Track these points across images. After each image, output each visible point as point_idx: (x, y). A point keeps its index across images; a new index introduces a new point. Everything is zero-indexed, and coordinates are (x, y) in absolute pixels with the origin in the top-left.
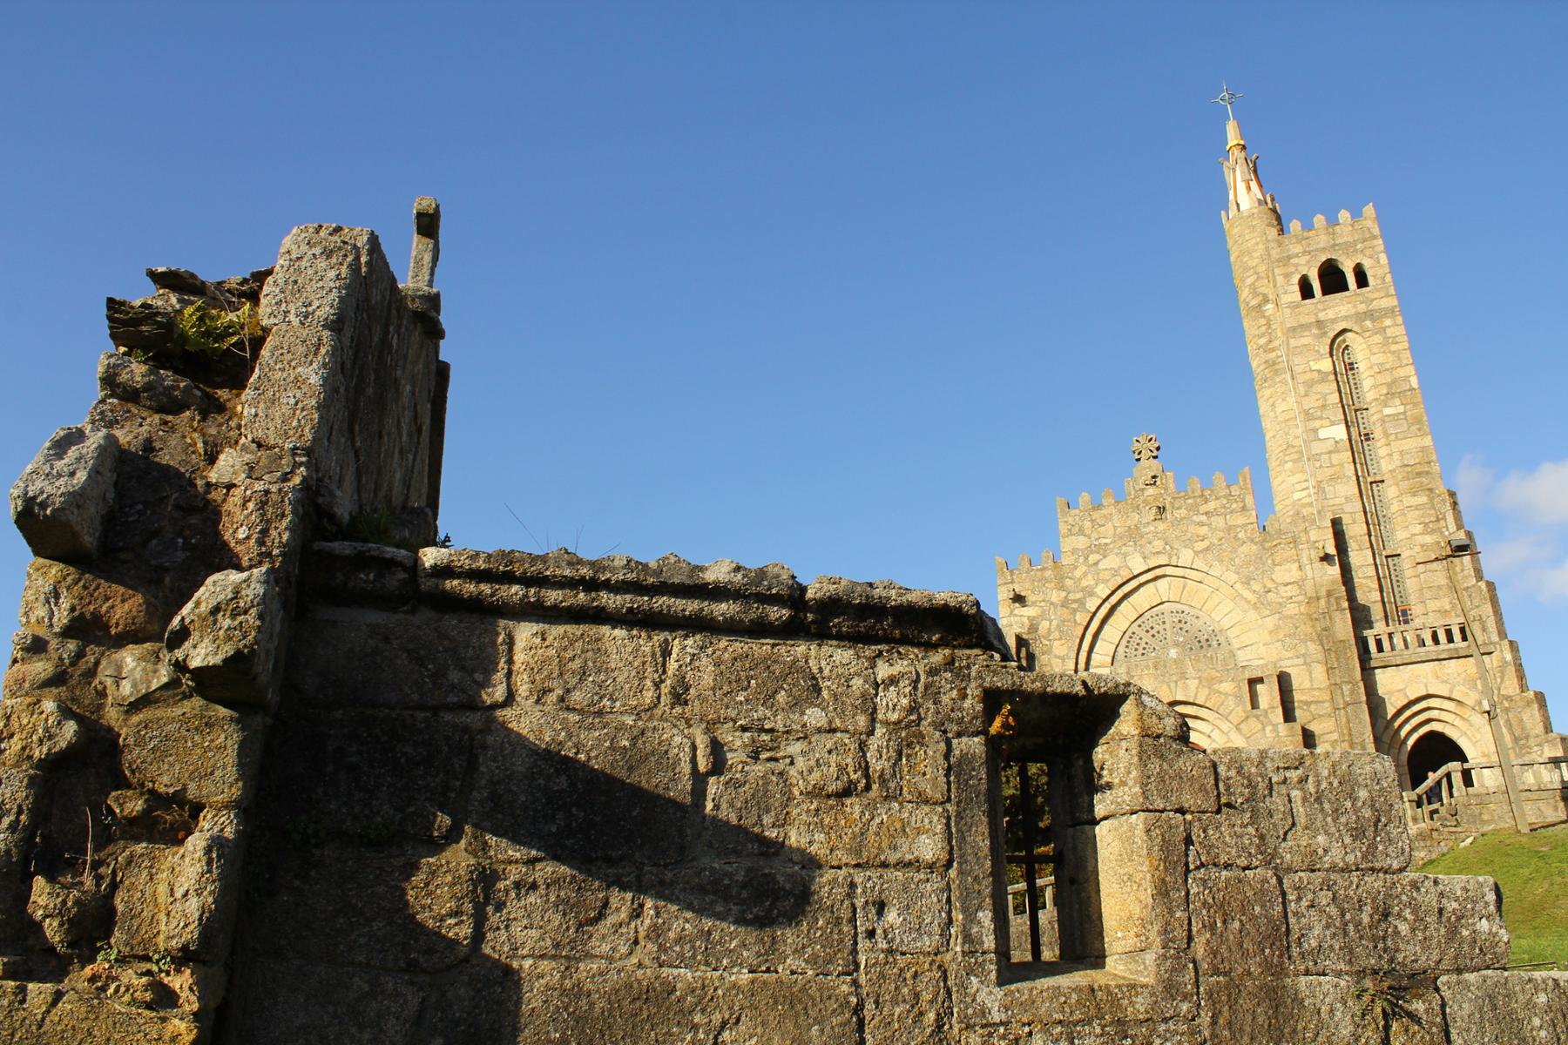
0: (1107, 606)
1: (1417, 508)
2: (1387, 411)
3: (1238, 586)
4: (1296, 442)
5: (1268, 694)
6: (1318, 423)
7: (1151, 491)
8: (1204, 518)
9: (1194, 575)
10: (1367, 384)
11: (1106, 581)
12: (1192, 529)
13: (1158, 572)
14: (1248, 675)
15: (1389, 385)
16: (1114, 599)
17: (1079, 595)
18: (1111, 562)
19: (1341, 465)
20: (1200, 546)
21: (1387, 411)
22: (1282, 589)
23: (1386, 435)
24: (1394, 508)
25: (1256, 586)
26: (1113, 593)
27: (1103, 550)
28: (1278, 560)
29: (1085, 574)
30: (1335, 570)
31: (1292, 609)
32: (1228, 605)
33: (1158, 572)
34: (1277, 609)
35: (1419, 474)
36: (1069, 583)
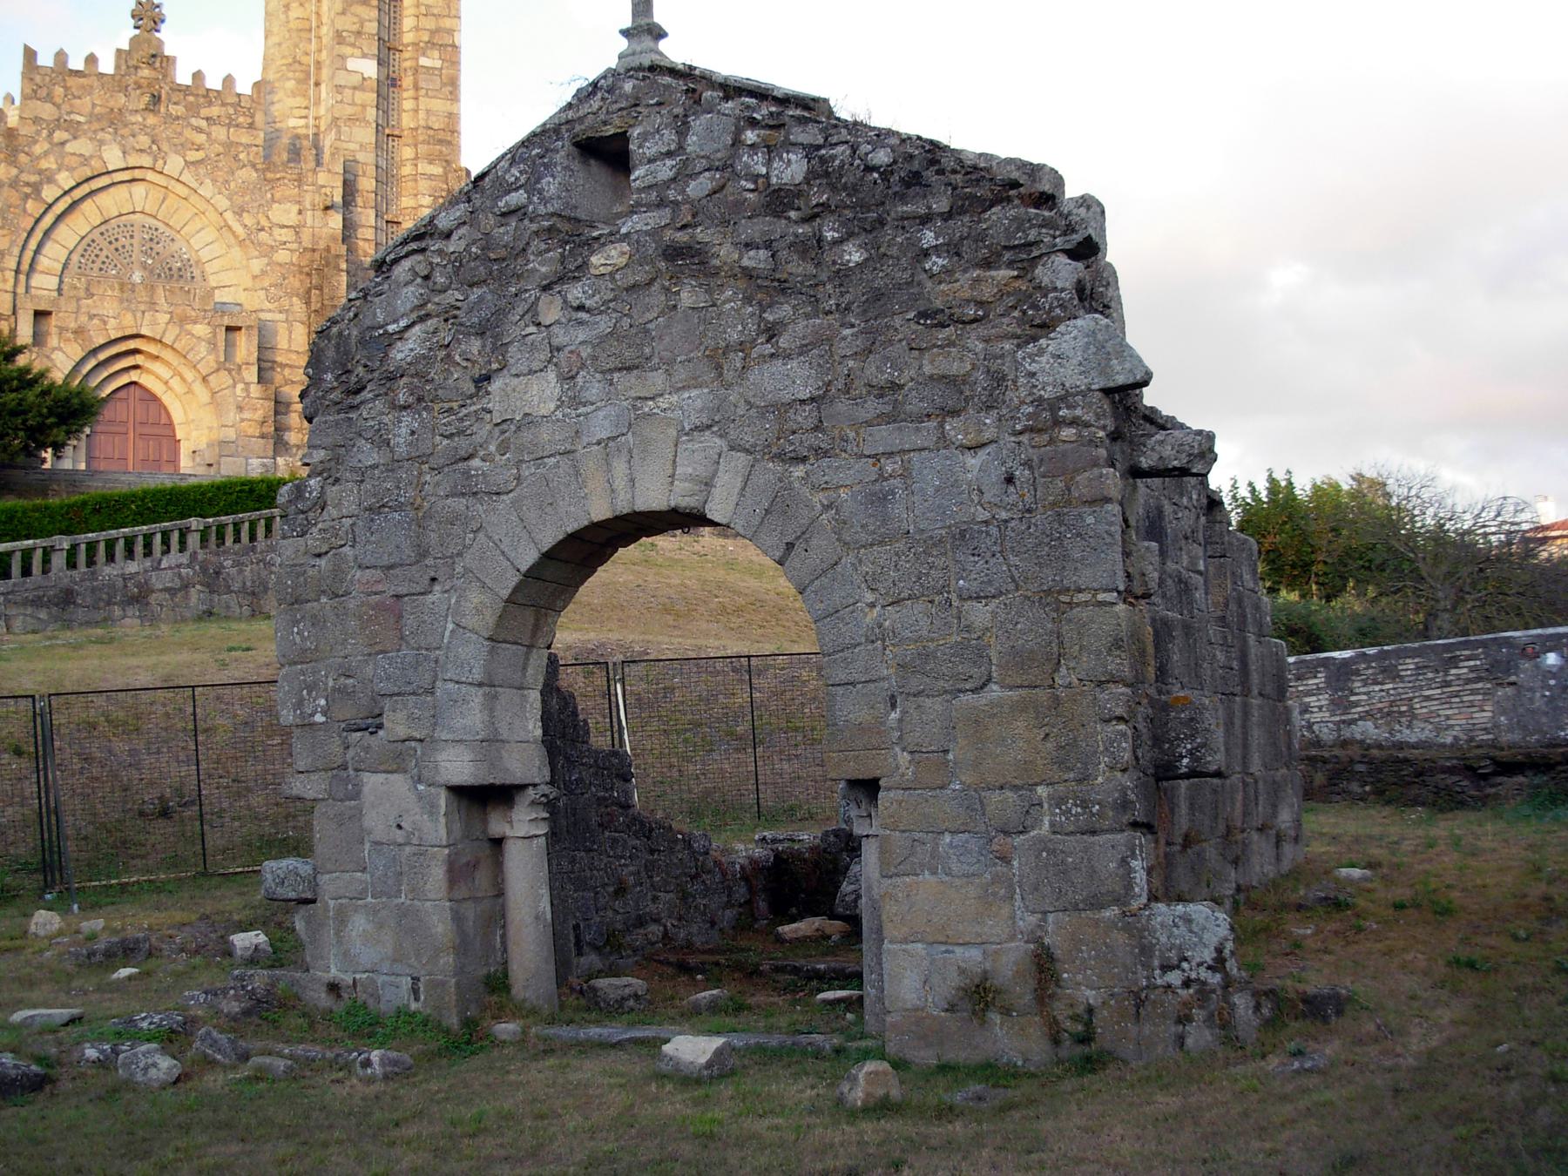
0: (68, 200)
1: (430, 177)
2: (423, 61)
3: (229, 215)
4: (304, 59)
5: (246, 347)
6: (348, 50)
7: (145, 72)
8: (203, 124)
9: (180, 189)
10: (408, 23)
11: (71, 169)
12: (188, 133)
13: (137, 174)
14: (227, 321)
15: (433, 32)
16: (77, 194)
17: (34, 178)
18: (81, 146)
19: (364, 106)
20: (193, 156)
21: (423, 61)
22: (277, 231)
23: (416, 88)
24: (407, 170)
25: (248, 219)
26: (78, 185)
27: (75, 130)
28: (278, 196)
29: (46, 154)
30: (336, 221)
31: (282, 256)
32: (209, 234)
33: (137, 174)
34: (268, 251)
35: (441, 142)
36: (22, 158)
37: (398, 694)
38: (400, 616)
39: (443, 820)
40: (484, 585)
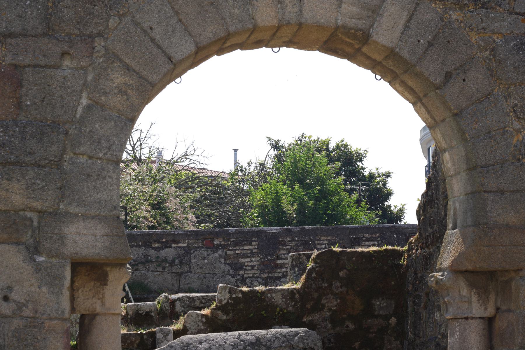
37: (15, 163)
38: (20, 85)
39: (66, 293)
40: (128, 68)
